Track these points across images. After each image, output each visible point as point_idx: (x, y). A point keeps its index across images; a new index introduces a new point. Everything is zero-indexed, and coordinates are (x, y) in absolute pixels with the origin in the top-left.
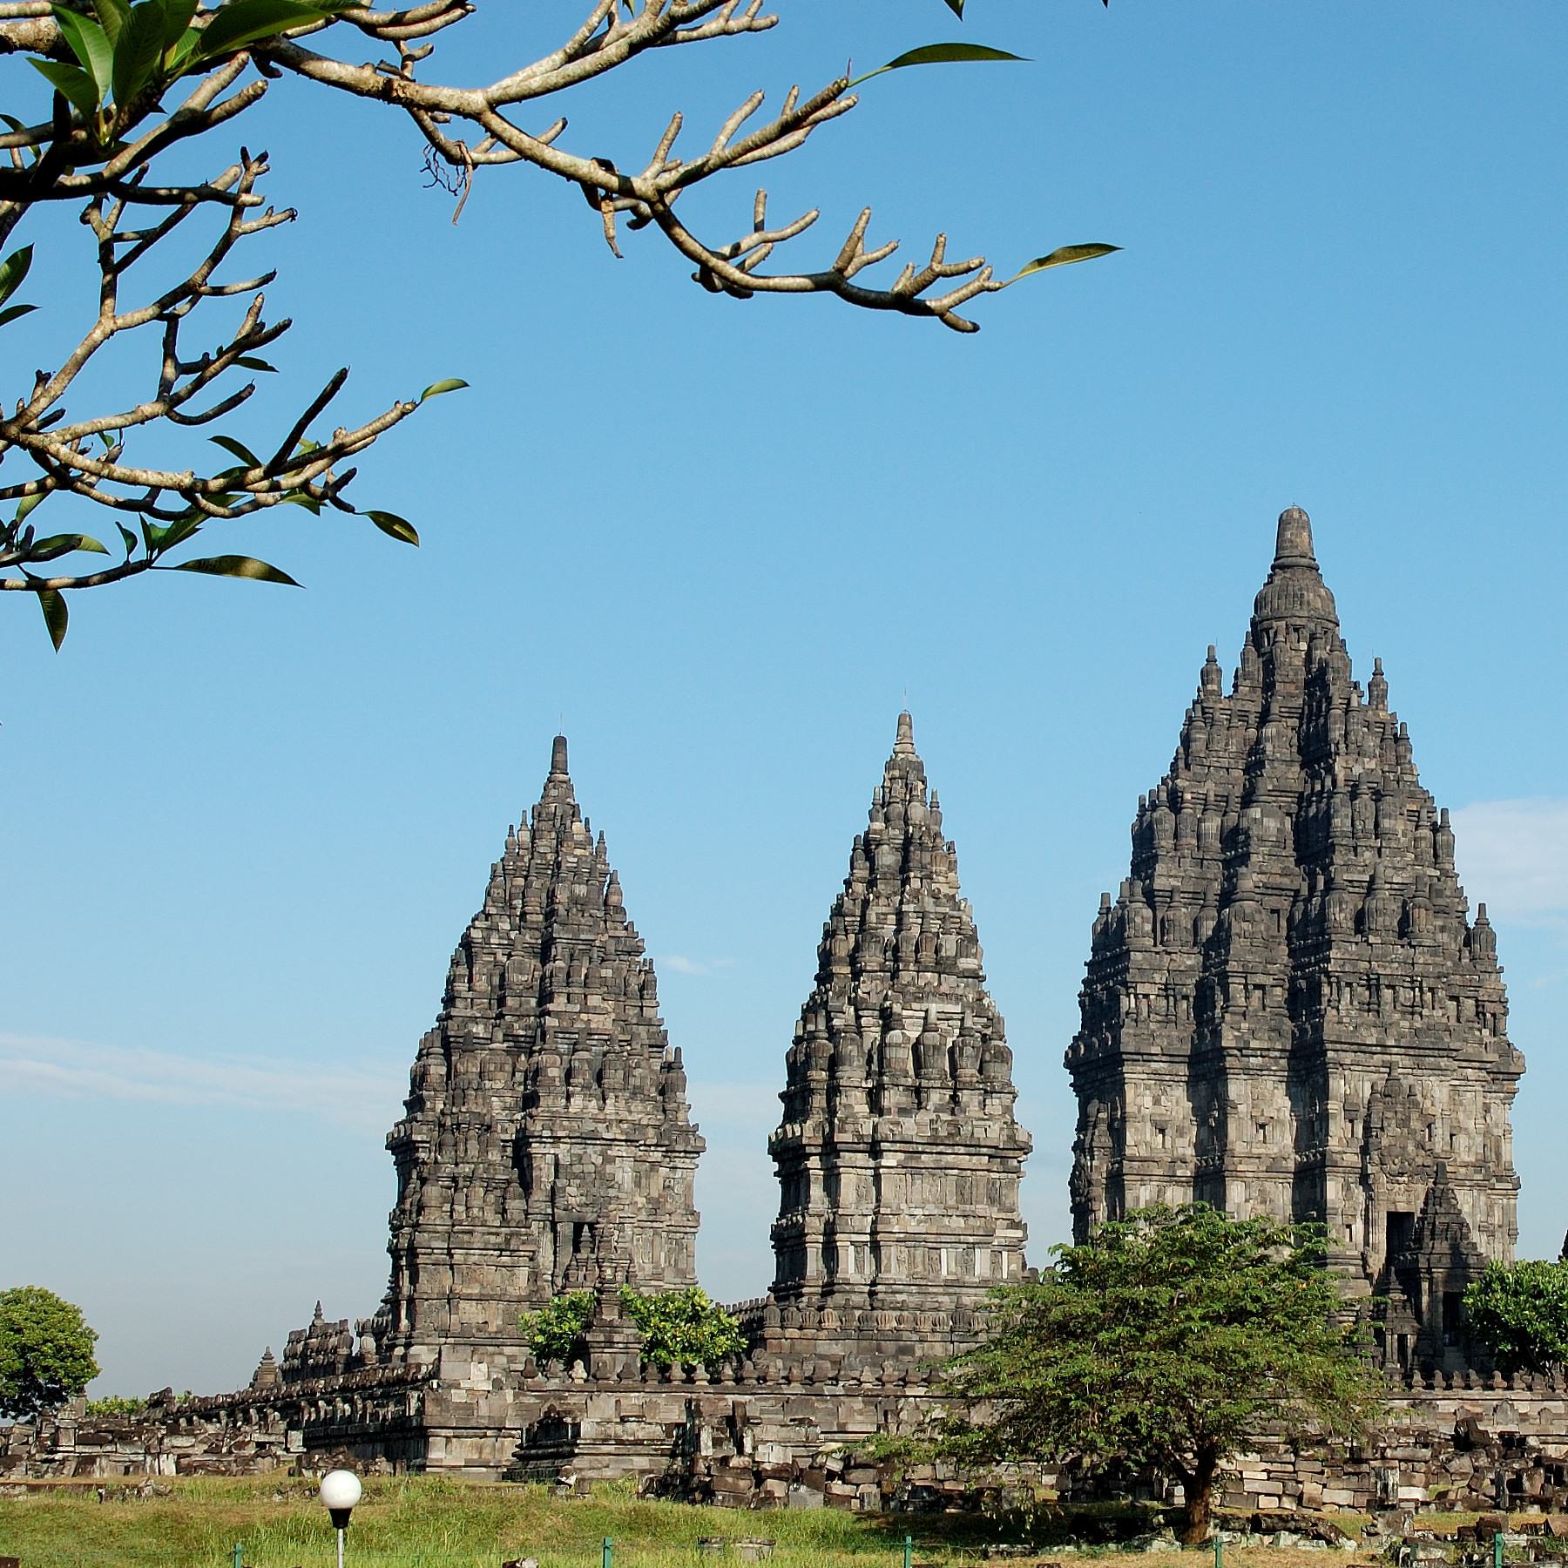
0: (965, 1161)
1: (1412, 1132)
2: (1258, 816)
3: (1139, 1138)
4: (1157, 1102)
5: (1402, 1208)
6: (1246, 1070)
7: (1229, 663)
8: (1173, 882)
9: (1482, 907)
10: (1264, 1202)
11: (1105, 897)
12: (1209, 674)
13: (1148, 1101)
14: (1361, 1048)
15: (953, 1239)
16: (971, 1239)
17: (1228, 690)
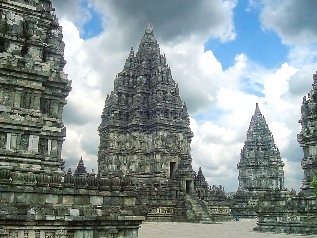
0: (28, 84)
1: (176, 144)
2: (142, 78)
3: (113, 145)
4: (118, 137)
5: (174, 161)
6: (138, 130)
7: (136, 51)
8: (123, 91)
9: (185, 103)
10: (141, 160)
11: (108, 95)
12: (132, 52)
13: (116, 137)
14: (165, 125)
15: (15, 127)
16: (27, 129)
17: (135, 56)
